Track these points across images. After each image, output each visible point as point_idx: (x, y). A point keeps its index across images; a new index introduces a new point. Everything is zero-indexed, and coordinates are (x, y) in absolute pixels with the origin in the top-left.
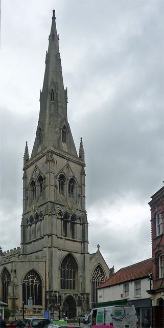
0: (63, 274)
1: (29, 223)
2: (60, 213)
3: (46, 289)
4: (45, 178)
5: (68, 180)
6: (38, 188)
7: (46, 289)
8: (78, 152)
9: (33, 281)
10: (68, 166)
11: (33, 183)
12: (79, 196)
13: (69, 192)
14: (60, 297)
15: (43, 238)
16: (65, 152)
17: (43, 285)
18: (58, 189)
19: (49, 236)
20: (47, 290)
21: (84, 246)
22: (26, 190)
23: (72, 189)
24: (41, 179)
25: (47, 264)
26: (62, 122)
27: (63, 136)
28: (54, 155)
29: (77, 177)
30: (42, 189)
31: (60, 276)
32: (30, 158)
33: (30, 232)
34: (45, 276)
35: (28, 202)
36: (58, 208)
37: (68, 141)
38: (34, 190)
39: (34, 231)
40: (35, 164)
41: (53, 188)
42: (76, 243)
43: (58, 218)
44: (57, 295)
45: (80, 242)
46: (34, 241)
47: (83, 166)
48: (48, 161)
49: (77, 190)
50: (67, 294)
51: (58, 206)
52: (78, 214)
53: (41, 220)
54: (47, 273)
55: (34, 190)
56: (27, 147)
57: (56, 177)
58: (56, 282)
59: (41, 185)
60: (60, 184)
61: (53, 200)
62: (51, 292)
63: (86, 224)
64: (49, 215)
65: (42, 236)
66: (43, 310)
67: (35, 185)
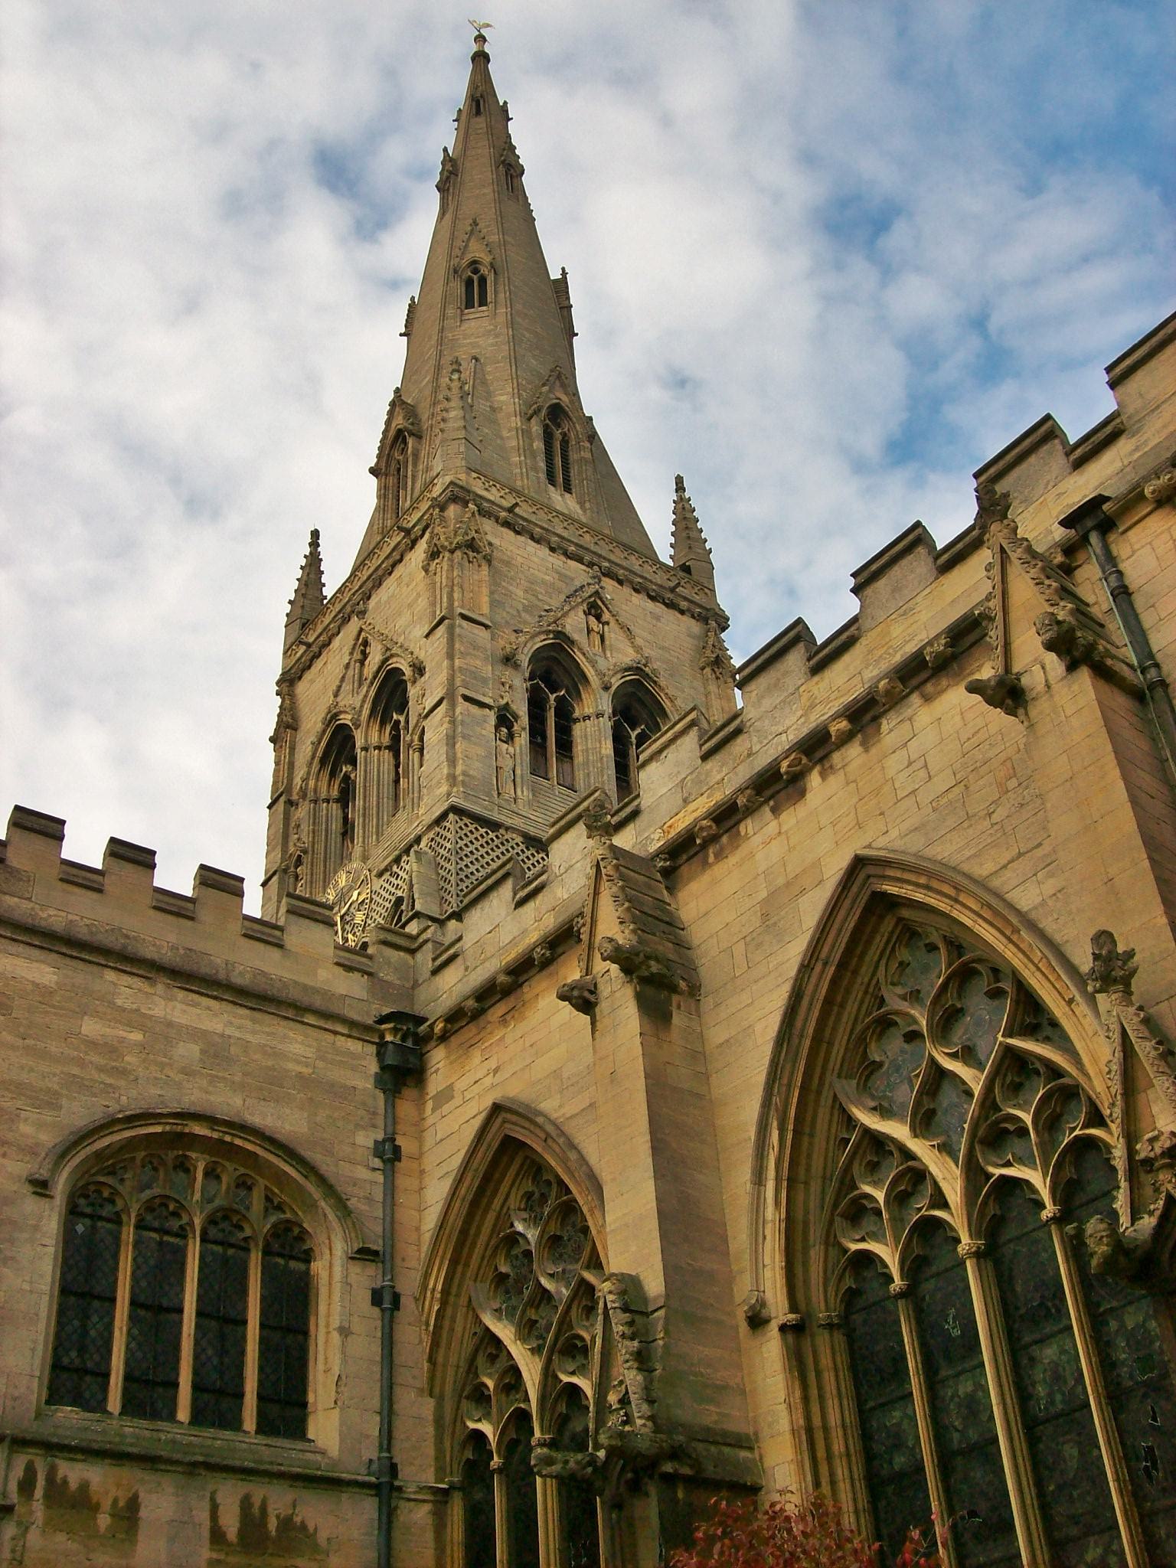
6: (372, 765)
11: (339, 746)
22: (283, 799)
40: (355, 624)
59: (394, 747)
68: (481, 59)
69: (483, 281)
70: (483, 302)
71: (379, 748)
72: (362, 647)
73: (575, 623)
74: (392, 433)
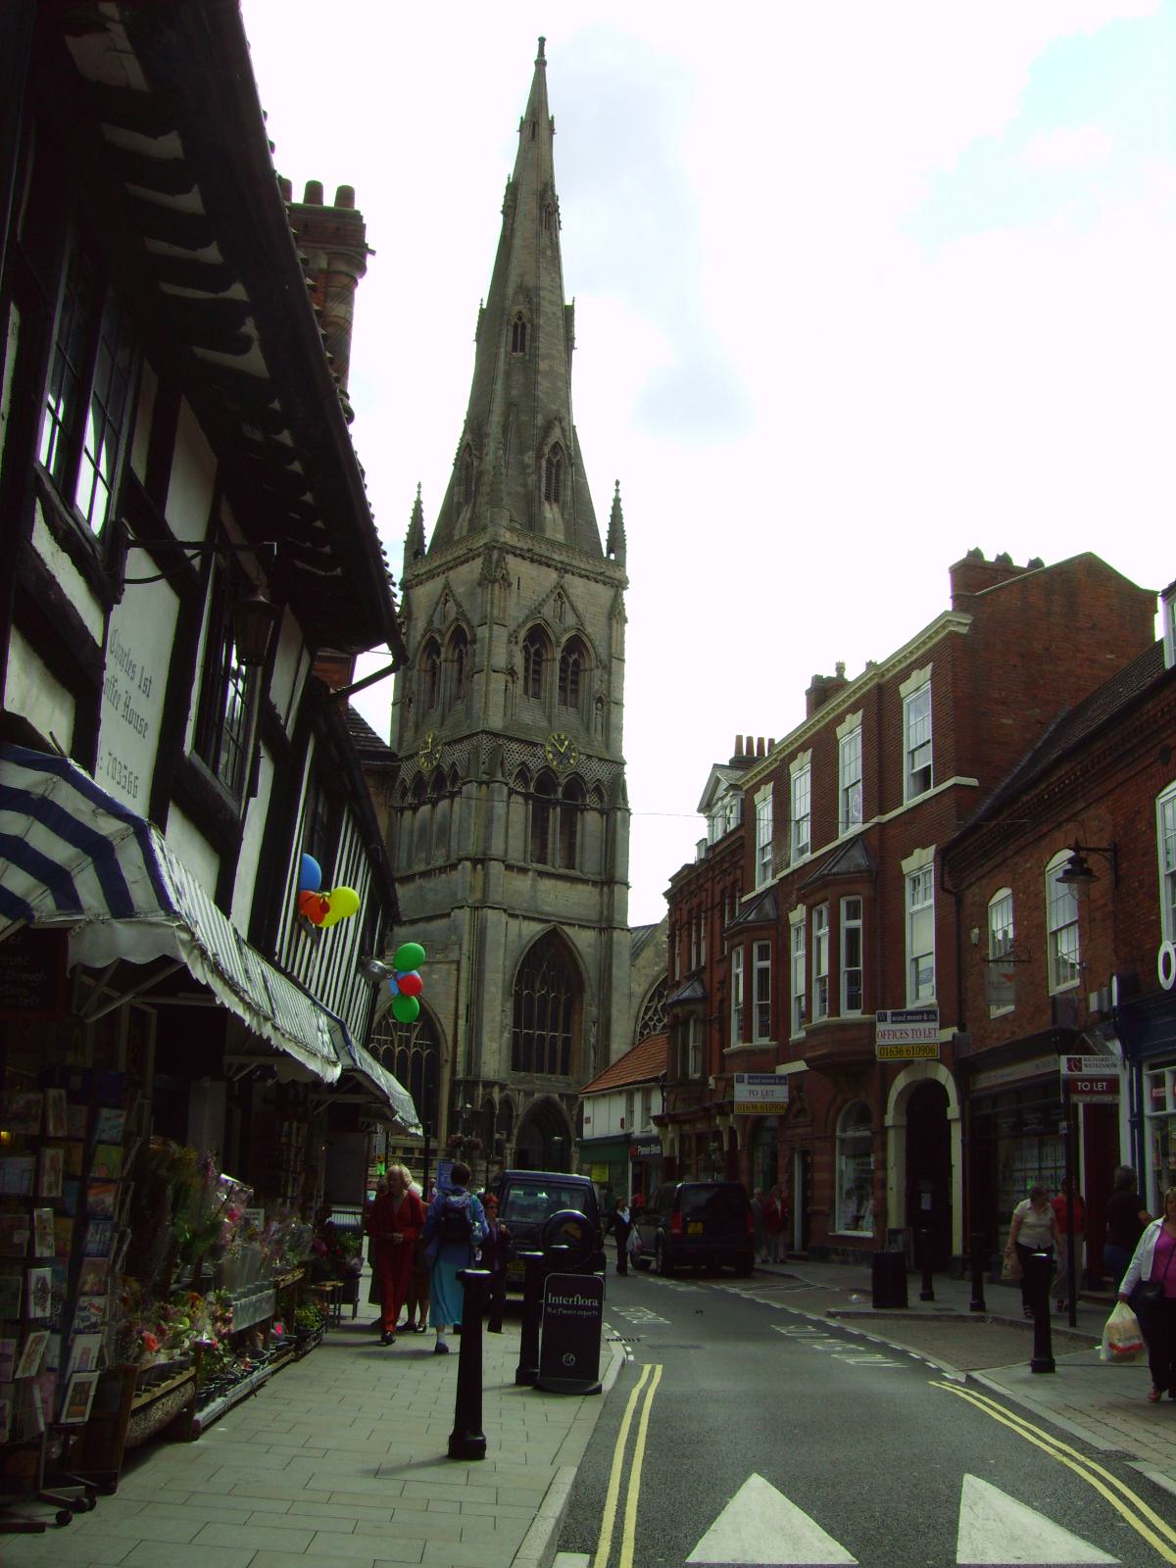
0: (523, 1012)
1: (409, 799)
2: (523, 774)
3: (454, 1072)
4: (474, 642)
5: (558, 644)
7: (454, 1072)
8: (604, 536)
9: (408, 1039)
10: (561, 593)
12: (600, 700)
13: (562, 688)
14: (507, 1103)
15: (454, 867)
16: (552, 543)
17: (446, 1054)
18: (521, 682)
19: (475, 861)
20: (460, 1076)
21: (612, 893)
23: (576, 674)
24: (461, 638)
25: (464, 975)
26: (548, 428)
27: (549, 478)
28: (510, 558)
29: (595, 630)
30: (464, 676)
31: (509, 1021)
32: (428, 541)
33: (411, 835)
34: (452, 1024)
35: (411, 717)
36: (515, 754)
37: (567, 495)
38: (434, 670)
39: (424, 830)
40: (442, 577)
41: (499, 681)
42: (580, 887)
43: (511, 792)
44: (496, 1095)
45: (595, 883)
46: (424, 874)
47: (619, 585)
48: (486, 580)
49: (594, 681)
51: (515, 746)
52: (596, 771)
53: (452, 796)
54: (462, 1011)
55: (434, 670)
56: (418, 503)
57: (512, 638)
58: (495, 1046)
59: (460, 660)
60: (527, 660)
61: (496, 721)
62: (475, 1083)
63: (619, 814)
64: (480, 783)
65: (453, 860)
67: (438, 654)
68: (537, 128)
69: (524, 326)
70: (523, 349)
71: (452, 661)
72: (447, 593)
73: (548, 611)
74: (464, 443)
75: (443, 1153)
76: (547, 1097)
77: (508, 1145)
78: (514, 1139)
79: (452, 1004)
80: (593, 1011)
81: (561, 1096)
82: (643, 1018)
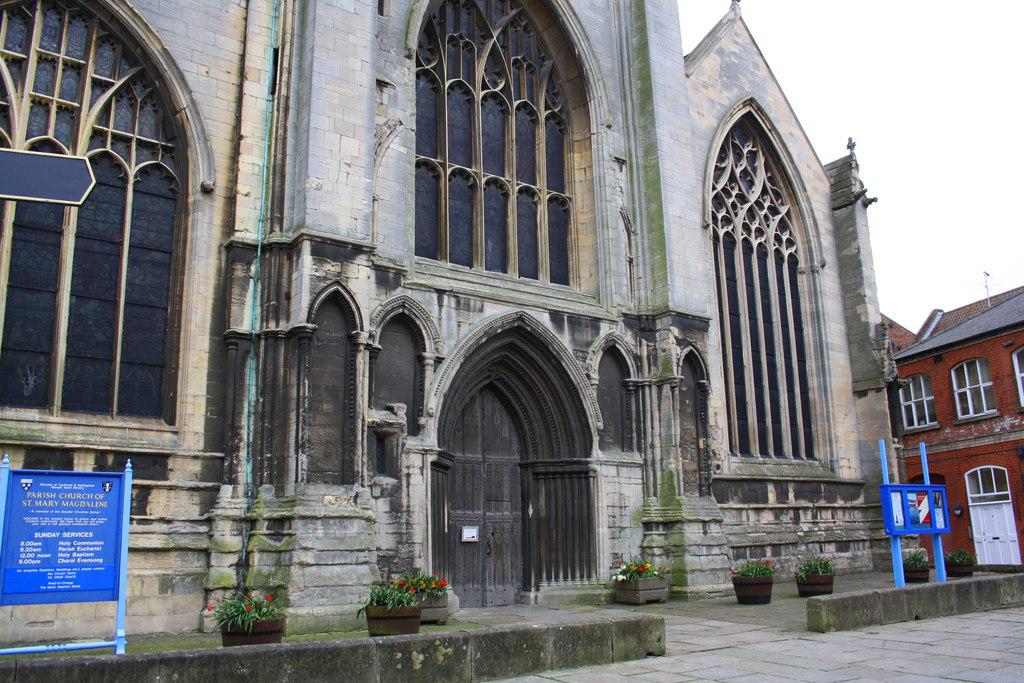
3: (229, 225)
7: (229, 225)
14: (404, 324)
17: (205, 168)
20: (250, 230)
50: (494, 312)
62: (291, 249)
66: (184, 472)
75: (196, 467)
76: (521, 318)
77: (411, 442)
78: (431, 426)
79: (237, 48)
80: (608, 141)
81: (556, 316)
82: (714, 188)
